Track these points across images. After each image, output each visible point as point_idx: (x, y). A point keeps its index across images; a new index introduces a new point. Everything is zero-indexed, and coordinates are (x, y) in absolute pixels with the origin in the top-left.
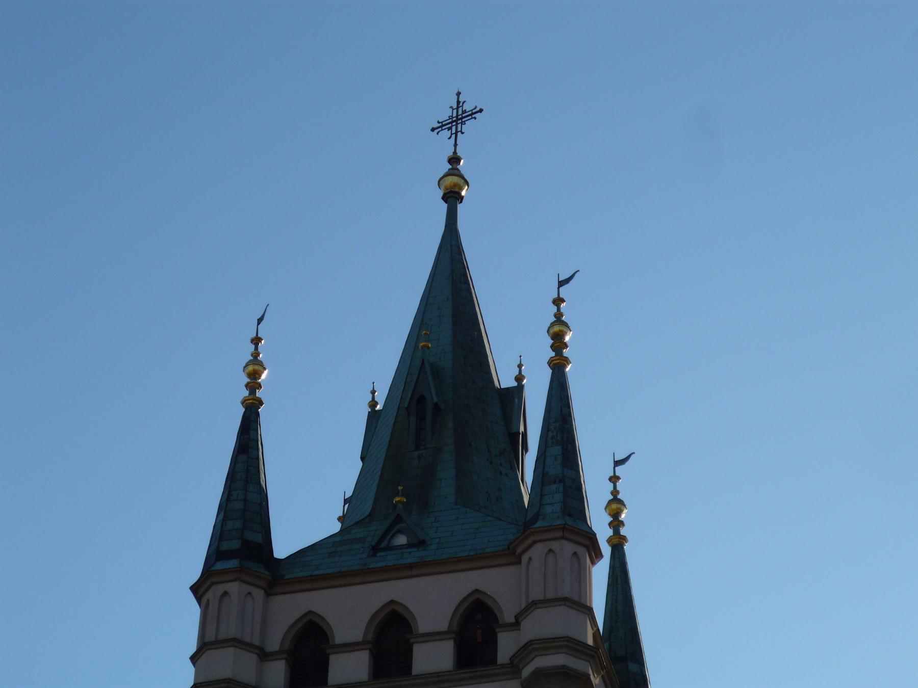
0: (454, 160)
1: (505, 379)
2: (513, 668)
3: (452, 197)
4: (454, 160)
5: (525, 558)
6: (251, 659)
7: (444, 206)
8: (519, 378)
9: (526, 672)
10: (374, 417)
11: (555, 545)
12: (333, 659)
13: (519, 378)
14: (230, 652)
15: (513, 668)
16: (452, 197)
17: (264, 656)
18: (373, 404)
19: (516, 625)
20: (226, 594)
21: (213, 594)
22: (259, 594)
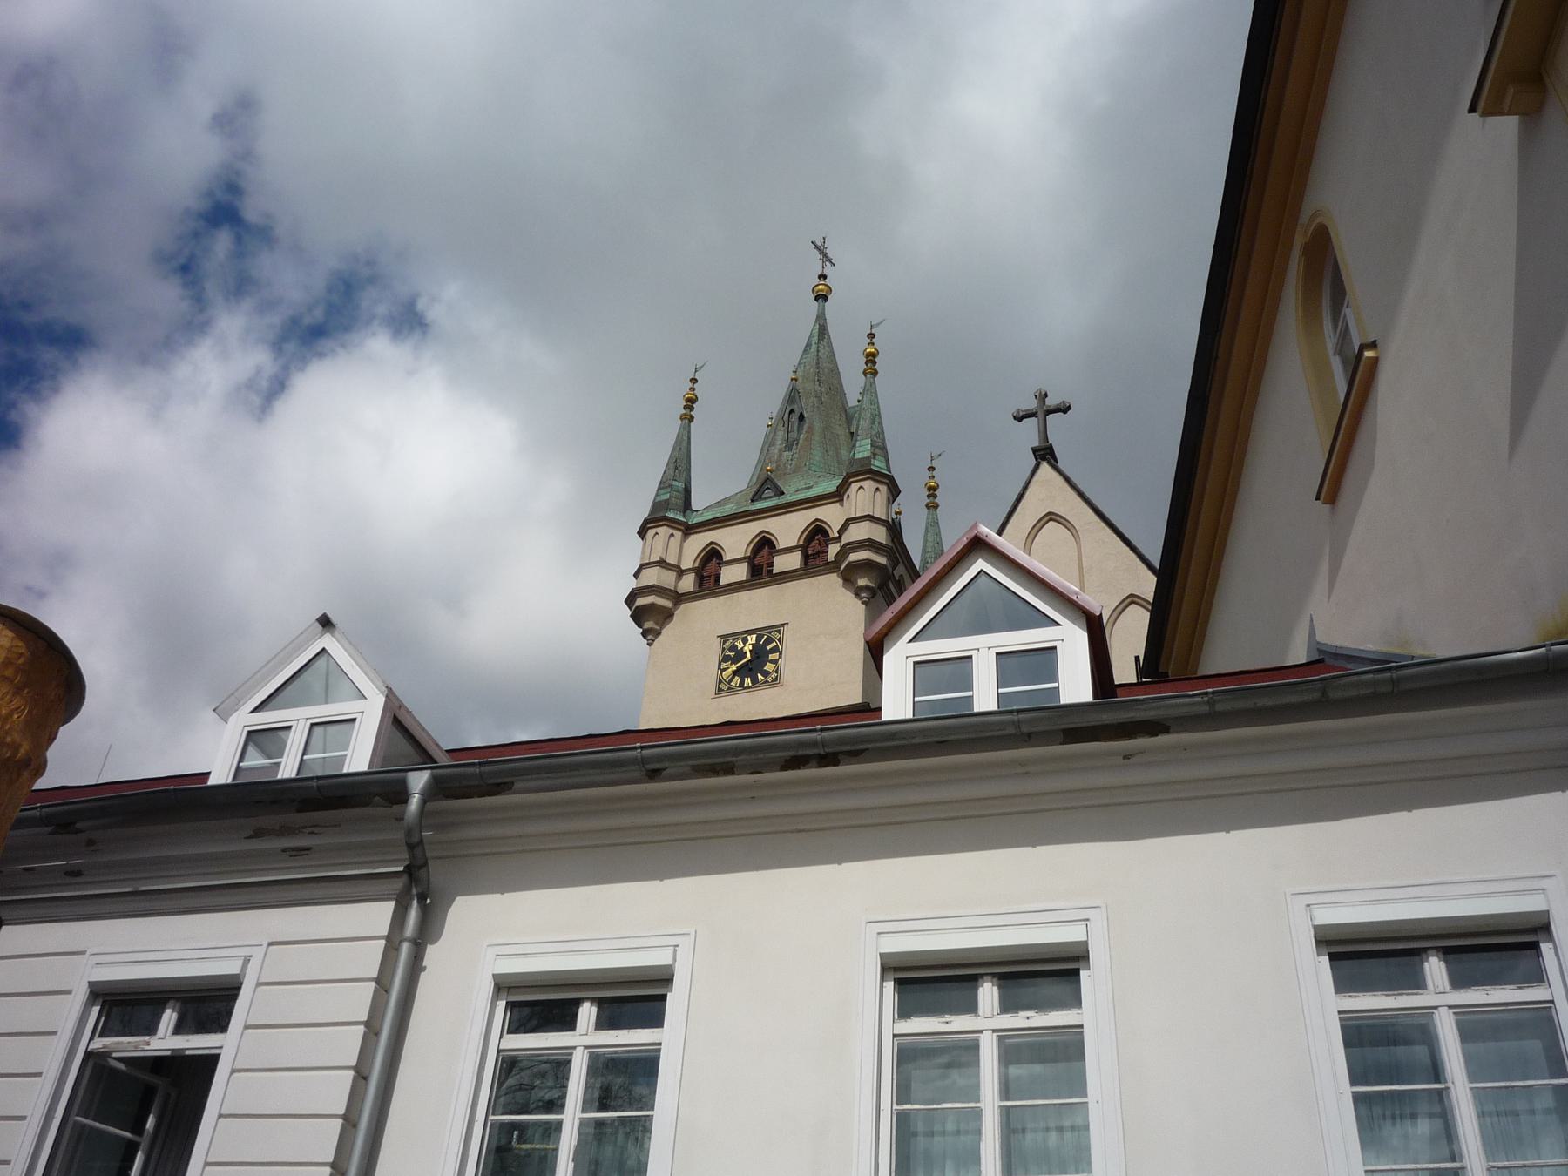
17: (681, 573)
20: (657, 533)
22: (678, 534)
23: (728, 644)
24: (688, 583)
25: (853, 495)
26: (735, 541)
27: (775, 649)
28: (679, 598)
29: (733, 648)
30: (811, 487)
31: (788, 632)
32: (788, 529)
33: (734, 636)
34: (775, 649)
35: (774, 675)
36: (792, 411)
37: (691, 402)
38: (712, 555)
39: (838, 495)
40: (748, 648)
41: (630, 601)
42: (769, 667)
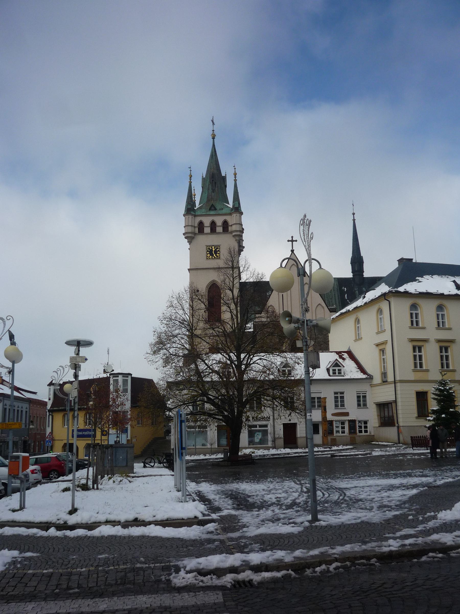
0: (213, 131)
1: (223, 175)
2: (231, 232)
3: (213, 138)
4: (213, 131)
5: (232, 215)
6: (193, 228)
7: (212, 139)
8: (226, 175)
9: (234, 234)
10: (203, 179)
11: (237, 214)
12: (205, 228)
13: (226, 175)
14: (190, 227)
15: (231, 232)
16: (213, 138)
18: (203, 176)
19: (231, 226)
21: (186, 216)
23: (208, 248)
24: (197, 230)
25: (234, 217)
26: (207, 221)
27: (218, 251)
28: (195, 234)
29: (209, 249)
30: (222, 209)
31: (221, 247)
32: (219, 221)
33: (209, 246)
34: (218, 251)
35: (219, 257)
36: (213, 180)
37: (191, 177)
38: (201, 224)
39: (230, 214)
40: (214, 249)
41: (184, 234)
42: (218, 255)
